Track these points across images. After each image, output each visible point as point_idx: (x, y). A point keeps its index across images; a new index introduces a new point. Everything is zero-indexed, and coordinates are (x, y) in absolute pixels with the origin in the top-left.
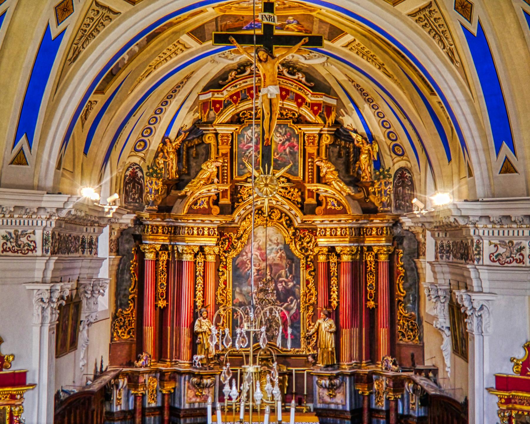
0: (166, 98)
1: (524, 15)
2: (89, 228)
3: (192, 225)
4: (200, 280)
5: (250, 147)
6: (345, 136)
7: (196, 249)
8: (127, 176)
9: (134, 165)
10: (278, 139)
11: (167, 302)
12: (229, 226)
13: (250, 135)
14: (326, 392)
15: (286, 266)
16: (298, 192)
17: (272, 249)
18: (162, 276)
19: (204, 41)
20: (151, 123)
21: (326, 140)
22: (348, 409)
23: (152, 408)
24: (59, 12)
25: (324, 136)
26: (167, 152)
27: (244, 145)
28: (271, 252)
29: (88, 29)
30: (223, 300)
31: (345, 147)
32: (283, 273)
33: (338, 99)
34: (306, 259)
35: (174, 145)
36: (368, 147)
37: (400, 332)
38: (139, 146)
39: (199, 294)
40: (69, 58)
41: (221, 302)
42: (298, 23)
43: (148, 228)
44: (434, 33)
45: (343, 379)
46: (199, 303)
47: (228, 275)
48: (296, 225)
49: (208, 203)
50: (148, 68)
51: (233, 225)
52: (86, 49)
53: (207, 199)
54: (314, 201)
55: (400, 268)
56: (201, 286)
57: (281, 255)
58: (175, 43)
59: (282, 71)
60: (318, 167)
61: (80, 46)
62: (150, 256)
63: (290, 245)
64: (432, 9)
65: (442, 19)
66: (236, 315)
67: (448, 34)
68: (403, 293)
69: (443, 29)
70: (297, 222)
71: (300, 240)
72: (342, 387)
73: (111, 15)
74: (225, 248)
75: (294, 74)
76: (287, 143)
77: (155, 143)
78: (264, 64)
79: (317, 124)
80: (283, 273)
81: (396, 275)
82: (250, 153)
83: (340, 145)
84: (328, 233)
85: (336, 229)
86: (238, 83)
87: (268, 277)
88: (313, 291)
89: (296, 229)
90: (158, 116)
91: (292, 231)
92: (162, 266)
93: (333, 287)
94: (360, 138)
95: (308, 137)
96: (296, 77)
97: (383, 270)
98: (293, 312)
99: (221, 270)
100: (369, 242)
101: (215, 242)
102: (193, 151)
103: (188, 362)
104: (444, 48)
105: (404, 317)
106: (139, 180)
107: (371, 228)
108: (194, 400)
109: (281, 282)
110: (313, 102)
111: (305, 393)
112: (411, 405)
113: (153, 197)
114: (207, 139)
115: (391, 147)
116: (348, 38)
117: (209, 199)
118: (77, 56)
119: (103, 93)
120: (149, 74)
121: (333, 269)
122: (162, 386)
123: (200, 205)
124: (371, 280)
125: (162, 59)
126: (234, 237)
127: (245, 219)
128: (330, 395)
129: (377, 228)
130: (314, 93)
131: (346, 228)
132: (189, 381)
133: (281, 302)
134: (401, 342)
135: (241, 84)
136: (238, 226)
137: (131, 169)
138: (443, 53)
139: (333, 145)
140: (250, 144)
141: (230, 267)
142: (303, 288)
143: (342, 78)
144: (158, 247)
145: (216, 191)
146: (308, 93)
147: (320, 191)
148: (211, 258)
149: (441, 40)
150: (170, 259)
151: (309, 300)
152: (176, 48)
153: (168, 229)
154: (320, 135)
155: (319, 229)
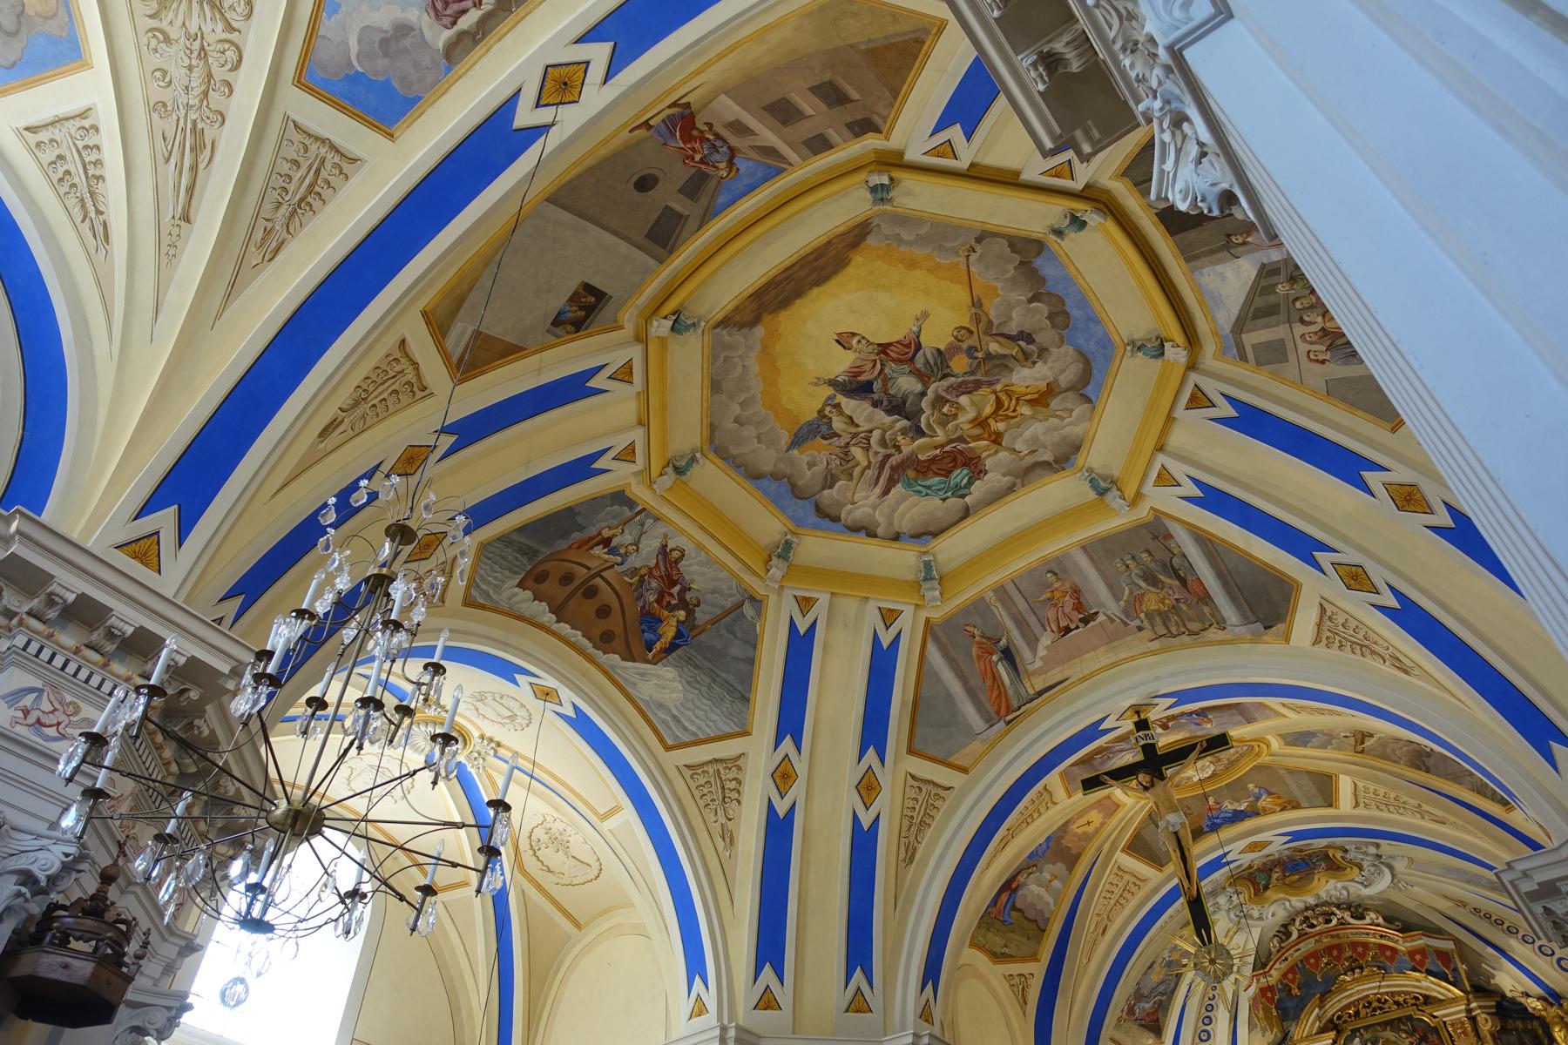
0: (1203, 1010)
1: (1432, 534)
19: (1162, 866)
24: (864, 793)
25: (1478, 1018)
29: (915, 814)
31: (1526, 1031)
33: (1457, 941)
36: (1554, 1011)
40: (902, 856)
42: (1270, 794)
44: (1358, 647)
50: (1096, 919)
52: (923, 844)
58: (1115, 871)
61: (912, 839)
64: (1329, 613)
65: (1351, 619)
67: (1373, 636)
69: (1362, 633)
73: (942, 793)
75: (1362, 917)
78: (1151, 790)
79: (1454, 1001)
83: (1516, 1029)
86: (1287, 954)
94: (1538, 1005)
95: (1452, 1025)
104: (1385, 662)
110: (1410, 949)
116: (1345, 785)
118: (913, 856)
119: (1037, 960)
125: (1112, 902)
130: (1405, 935)
138: (1388, 669)
139: (1503, 1030)
143: (1444, 905)
146: (1397, 938)
149: (1373, 652)
152: (1124, 881)
154: (1473, 1020)
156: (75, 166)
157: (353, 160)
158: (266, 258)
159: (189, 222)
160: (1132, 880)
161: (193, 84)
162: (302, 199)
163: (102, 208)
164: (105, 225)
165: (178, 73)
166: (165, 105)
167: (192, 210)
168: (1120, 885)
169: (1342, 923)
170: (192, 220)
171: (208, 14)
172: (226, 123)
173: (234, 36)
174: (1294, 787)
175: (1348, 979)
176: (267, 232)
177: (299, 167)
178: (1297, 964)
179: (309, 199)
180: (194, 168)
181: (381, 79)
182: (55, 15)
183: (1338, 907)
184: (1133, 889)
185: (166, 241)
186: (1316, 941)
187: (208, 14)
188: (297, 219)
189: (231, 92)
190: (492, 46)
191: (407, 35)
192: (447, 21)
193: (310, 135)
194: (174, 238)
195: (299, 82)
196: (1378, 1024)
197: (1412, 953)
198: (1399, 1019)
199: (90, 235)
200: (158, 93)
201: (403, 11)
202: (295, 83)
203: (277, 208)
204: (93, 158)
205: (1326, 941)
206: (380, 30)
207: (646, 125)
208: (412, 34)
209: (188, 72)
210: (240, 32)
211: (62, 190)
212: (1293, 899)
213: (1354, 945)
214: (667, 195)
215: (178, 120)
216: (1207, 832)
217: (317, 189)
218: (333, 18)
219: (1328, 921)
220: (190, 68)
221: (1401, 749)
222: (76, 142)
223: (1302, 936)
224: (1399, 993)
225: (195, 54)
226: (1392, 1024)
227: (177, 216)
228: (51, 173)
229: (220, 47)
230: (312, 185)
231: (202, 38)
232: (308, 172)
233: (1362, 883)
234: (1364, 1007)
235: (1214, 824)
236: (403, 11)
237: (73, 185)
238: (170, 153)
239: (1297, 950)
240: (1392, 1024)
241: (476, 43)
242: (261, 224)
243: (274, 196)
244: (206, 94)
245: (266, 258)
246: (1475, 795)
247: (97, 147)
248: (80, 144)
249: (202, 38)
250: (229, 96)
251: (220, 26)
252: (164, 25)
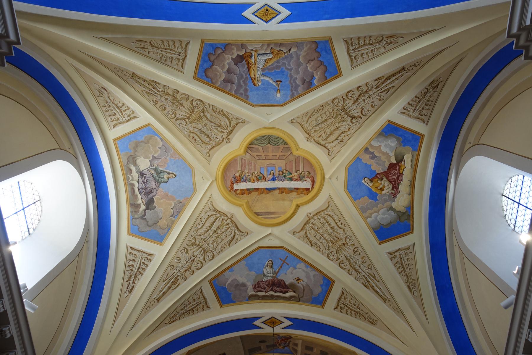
156: (136, 266)
157: (208, 307)
158: (169, 323)
159: (158, 302)
161: (185, 267)
162: (189, 310)
163: (136, 282)
164: (133, 287)
165: (183, 261)
166: (174, 267)
167: (161, 299)
170: (159, 302)
171: (201, 253)
172: (186, 281)
173: (204, 262)
176: (175, 315)
177: (194, 302)
179: (190, 311)
180: (169, 288)
181: (230, 292)
182: (164, 229)
185: (148, 304)
187: (201, 253)
188: (184, 315)
189: (192, 274)
190: (262, 302)
191: (243, 287)
192: (256, 290)
193: (203, 295)
194: (151, 305)
195: (210, 282)
199: (126, 287)
200: (174, 263)
201: (247, 281)
202: (209, 281)
203: (182, 310)
204: (143, 267)
206: (238, 282)
207: (279, 335)
208: (245, 287)
209: (186, 263)
210: (206, 262)
211: (127, 269)
214: (263, 346)
215: (174, 273)
217: (194, 310)
218: (230, 272)
220: (187, 262)
222: (142, 260)
225: (190, 260)
227: (156, 299)
228: (127, 262)
229: (198, 262)
230: (193, 308)
231: (196, 257)
232: (195, 304)
236: (247, 281)
237: (132, 270)
238: (166, 280)
241: (259, 299)
242: (175, 312)
243: (183, 306)
244: (186, 271)
245: (169, 323)
247: (147, 265)
248: (143, 261)
249: (196, 257)
250: (191, 275)
251: (202, 258)
252: (189, 249)
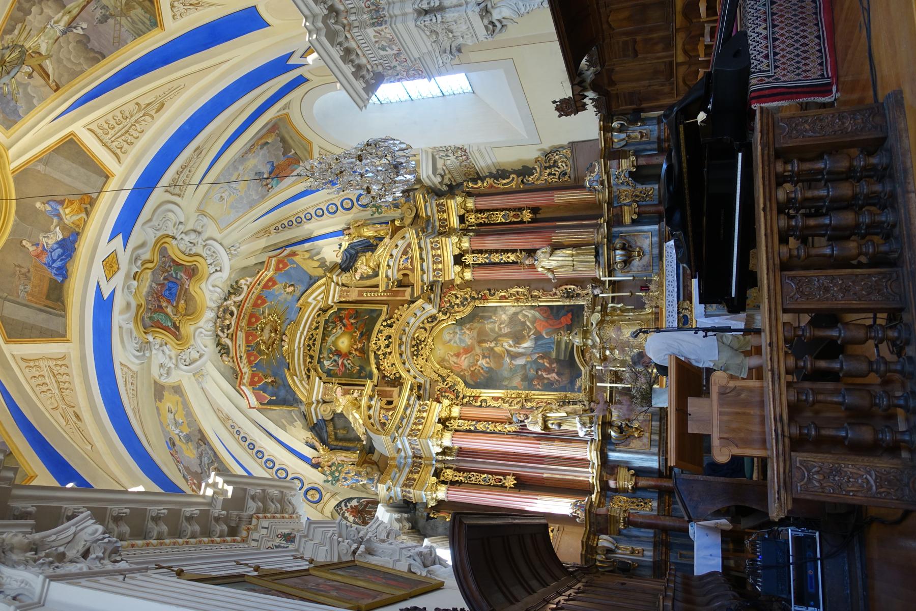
0: (250, 451)
2: (255, 536)
3: (409, 429)
4: (481, 426)
5: (343, 363)
6: (350, 262)
7: (440, 426)
8: (354, 520)
9: (341, 509)
10: (339, 331)
11: (509, 474)
12: (428, 391)
13: (329, 363)
14: (636, 262)
15: (481, 323)
16: (399, 309)
17: (459, 338)
18: (473, 478)
19: (64, 336)
20: (284, 475)
21: (345, 278)
22: (656, 227)
23: (658, 505)
25: (344, 282)
26: (328, 461)
27: (340, 370)
28: (464, 341)
30: (518, 403)
32: (489, 326)
34: (476, 299)
35: (323, 453)
37: (559, 179)
38: (312, 497)
39: (499, 428)
41: (520, 405)
42: (61, 203)
43: (405, 491)
45: (617, 237)
46: (509, 428)
47: (486, 394)
48: (434, 311)
49: (388, 410)
50: (57, 414)
51: (428, 387)
53: (383, 411)
54: (409, 290)
55: (485, 184)
56: (489, 425)
57: (468, 329)
58: (24, 365)
59: (235, 302)
60: (362, 278)
62: (442, 493)
63: (457, 318)
66: (538, 386)
68: (513, 178)
70: (431, 310)
71: (453, 307)
72: (627, 238)
74: (453, 397)
76: (344, 321)
77: (314, 477)
80: (489, 326)
81: (493, 190)
82: (349, 364)
84: (440, 266)
85: (433, 256)
86: (238, 355)
87: (493, 345)
88: (513, 291)
89: (439, 311)
90: (276, 467)
91: (441, 316)
92: (460, 477)
93: (502, 259)
96: (245, 288)
97: (484, 203)
98: (537, 314)
99: (479, 404)
100: (455, 222)
101: (438, 404)
102: (341, 433)
103: (589, 445)
105: (541, 175)
106: (361, 504)
107: (440, 220)
108: (645, 440)
109: (500, 329)
111: (632, 278)
112: (644, 139)
113: (363, 479)
114: (326, 413)
115: (361, 208)
117: (384, 409)
120: (77, 416)
121: (481, 259)
122: (624, 491)
123: (387, 420)
124: (499, 218)
126: (441, 385)
127: (421, 371)
128: (639, 255)
129: (439, 211)
131: (432, 243)
132: (617, 444)
133: (524, 329)
134: (572, 176)
135: (241, 352)
136: (429, 381)
137: (347, 514)
140: (340, 363)
141: (476, 392)
142: (508, 302)
143: (263, 242)
144: (434, 480)
145: (375, 399)
147: (390, 276)
148: (456, 411)
150: (454, 467)
151: (524, 295)
153: (416, 466)
154: (343, 285)
155: (435, 279)
160: (52, 363)
168: (45, 373)
169: (239, 305)
174: (67, 180)
175: (286, 347)
178: (248, 351)
183: (225, 300)
184: (63, 370)
186: (241, 330)
196: (322, 343)
197: (277, 269)
198: (324, 329)
205: (244, 324)
212: (201, 323)
213: (255, 305)
216: (63, 282)
219: (232, 314)
221: (70, 52)
223: (232, 337)
224: (311, 324)
226: (325, 336)
233: (216, 271)
234: (309, 350)
235: (58, 269)
239: (239, 347)
240: (325, 336)
246: (139, 39)
